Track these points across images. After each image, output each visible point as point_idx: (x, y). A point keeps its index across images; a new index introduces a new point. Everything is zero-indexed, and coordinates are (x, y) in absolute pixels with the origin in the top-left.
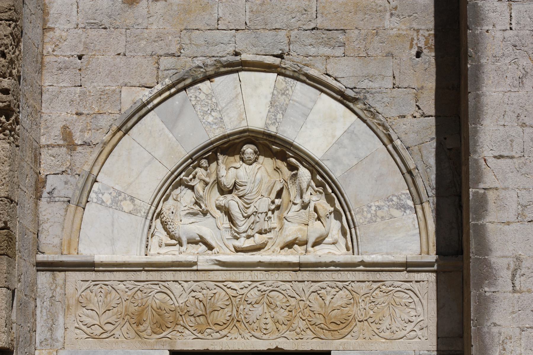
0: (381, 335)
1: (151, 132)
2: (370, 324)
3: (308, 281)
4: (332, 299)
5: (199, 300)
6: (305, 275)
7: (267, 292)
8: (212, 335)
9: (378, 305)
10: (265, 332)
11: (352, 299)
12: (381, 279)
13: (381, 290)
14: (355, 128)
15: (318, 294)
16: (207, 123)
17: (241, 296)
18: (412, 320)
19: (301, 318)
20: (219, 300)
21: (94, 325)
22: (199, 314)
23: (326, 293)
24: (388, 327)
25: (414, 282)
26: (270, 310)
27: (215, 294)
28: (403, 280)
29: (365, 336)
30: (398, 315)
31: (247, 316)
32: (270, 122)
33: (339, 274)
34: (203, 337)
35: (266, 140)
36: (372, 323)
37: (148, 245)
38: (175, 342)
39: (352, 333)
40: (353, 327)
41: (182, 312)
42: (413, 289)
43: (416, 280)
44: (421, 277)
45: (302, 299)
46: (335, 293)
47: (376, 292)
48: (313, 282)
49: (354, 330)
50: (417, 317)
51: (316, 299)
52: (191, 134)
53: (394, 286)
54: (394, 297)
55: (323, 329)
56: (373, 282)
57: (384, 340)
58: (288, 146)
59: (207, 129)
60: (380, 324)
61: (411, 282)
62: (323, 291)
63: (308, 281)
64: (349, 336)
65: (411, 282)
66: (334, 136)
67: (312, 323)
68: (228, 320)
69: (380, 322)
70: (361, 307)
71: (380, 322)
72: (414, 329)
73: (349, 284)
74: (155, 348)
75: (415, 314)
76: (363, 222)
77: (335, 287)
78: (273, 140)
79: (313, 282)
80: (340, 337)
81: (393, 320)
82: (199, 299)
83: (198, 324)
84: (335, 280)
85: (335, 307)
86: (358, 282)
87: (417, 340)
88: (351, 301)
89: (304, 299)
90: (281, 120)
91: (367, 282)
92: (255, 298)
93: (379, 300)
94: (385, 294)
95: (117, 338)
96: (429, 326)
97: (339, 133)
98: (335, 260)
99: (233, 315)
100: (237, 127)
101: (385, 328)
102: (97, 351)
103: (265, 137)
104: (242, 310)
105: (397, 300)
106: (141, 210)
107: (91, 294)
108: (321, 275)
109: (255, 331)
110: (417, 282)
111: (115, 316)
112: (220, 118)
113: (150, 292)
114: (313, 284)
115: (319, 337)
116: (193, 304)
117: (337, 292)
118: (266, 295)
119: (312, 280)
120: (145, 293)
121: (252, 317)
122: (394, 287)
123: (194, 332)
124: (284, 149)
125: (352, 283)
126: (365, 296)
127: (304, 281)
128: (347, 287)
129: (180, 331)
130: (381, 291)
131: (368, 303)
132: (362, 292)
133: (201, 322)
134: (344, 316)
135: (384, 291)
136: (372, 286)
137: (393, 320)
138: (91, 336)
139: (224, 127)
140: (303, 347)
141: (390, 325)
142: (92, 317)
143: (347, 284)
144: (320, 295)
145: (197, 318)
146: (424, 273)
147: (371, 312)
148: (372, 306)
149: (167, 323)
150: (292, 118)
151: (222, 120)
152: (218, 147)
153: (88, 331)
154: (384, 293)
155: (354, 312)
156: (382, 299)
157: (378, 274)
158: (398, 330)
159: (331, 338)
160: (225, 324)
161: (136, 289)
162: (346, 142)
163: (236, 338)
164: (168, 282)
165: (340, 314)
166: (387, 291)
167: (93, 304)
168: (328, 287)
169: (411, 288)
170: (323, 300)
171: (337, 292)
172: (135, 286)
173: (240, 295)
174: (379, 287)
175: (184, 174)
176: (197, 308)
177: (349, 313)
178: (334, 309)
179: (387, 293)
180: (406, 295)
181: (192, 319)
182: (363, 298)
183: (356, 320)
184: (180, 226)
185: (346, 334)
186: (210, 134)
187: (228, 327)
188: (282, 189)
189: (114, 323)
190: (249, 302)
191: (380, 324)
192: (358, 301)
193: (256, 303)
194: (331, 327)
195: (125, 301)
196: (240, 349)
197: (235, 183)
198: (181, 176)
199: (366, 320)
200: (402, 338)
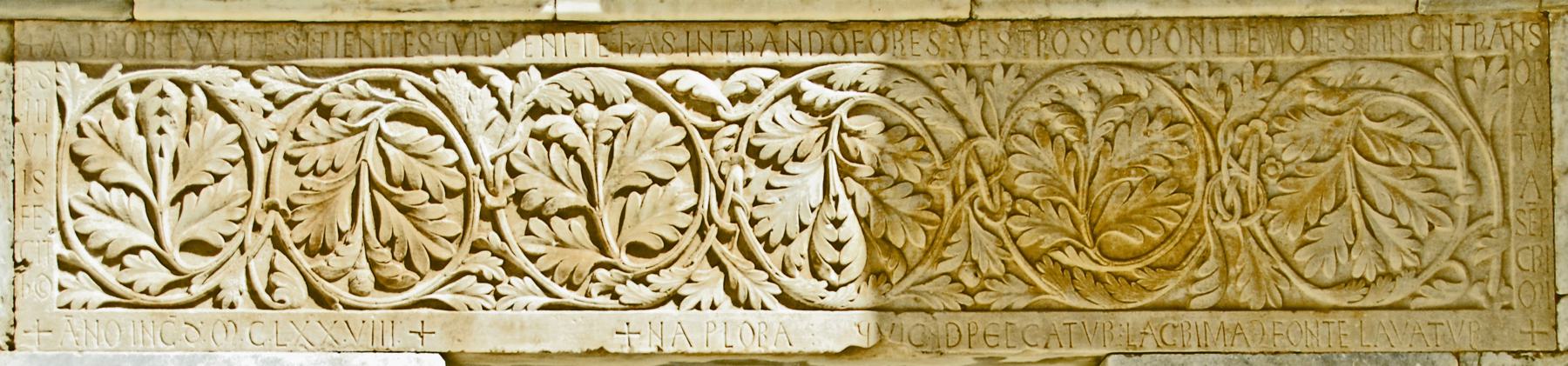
5: (564, 147)
7: (842, 111)
8: (619, 289)
10: (833, 277)
17: (734, 129)
20: (643, 146)
21: (135, 250)
22: (564, 205)
26: (854, 187)
27: (626, 120)
31: (758, 212)
33: (1136, 34)
34: (586, 302)
38: (469, 321)
41: (495, 194)
44: (1480, 38)
68: (683, 231)
74: (388, 344)
82: (565, 140)
83: (562, 244)
92: (792, 134)
95: (232, 306)
99: (703, 211)
102: (153, 357)
104: (740, 185)
107: (117, 122)
109: (796, 273)
111: (223, 215)
113: (366, 114)
116: (538, 163)
118: (836, 126)
120: (344, 118)
121: (778, 219)
123: (546, 281)
129: (488, 276)
133: (576, 240)
138: (117, 300)
142: (129, 220)
145: (556, 221)
149: (433, 240)
153: (110, 275)
160: (668, 246)
161: (306, 101)
163: (713, 307)
164: (437, 74)
167: (131, 161)
172: (301, 89)
173: (729, 123)
176: (556, 178)
181: (536, 224)
187: (683, 260)
189: (217, 241)
190: (764, 155)
193: (796, 158)
195: (263, 151)
196: (734, 350)
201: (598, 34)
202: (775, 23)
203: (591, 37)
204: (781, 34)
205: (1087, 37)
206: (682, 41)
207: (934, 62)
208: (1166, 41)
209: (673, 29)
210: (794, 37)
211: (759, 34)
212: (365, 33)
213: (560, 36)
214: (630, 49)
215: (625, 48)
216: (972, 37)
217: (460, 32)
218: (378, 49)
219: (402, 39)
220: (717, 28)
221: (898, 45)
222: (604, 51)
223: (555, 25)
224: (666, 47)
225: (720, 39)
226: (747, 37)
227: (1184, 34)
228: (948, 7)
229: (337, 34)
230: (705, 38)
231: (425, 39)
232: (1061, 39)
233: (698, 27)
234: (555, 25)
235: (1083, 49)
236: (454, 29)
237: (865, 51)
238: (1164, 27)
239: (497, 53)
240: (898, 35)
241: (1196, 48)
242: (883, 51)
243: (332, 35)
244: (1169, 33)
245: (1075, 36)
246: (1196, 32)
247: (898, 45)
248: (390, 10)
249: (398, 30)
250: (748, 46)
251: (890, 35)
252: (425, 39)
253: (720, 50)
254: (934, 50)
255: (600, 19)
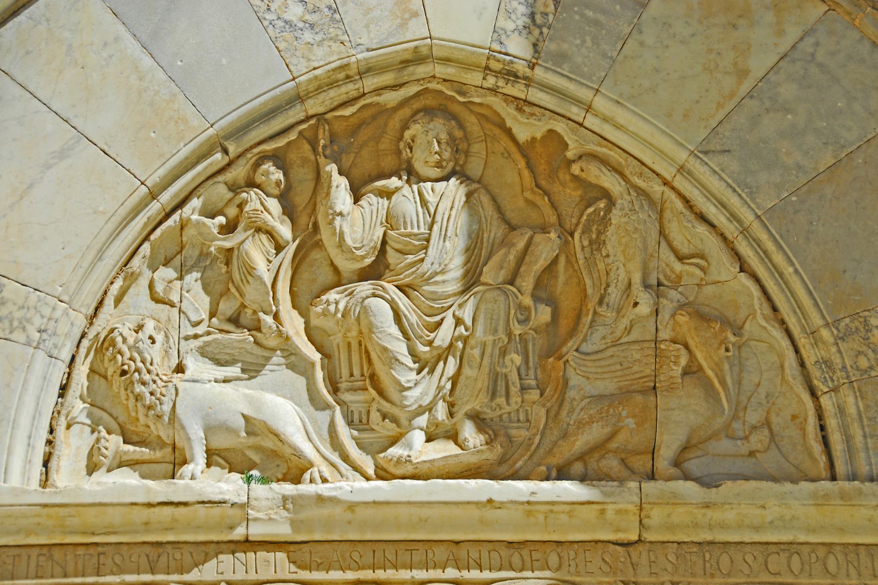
1: (70, 47)
14: (817, 44)
16: (280, 23)
32: (510, 26)
35: (494, 91)
37: (50, 453)
52: (224, 61)
58: (576, 112)
59: (282, 46)
66: (742, 73)
76: (871, 368)
78: (517, 90)
90: (551, 17)
97: (759, 64)
100: (393, 41)
103: (491, 81)
106: (29, 321)
112: (330, 8)
124: (560, 127)
139: (346, 38)
150: (590, 14)
151: (337, 16)
152: (320, 117)
162: (787, 91)
175: (196, 203)
184: (181, 386)
186: (294, 61)
188: (555, 261)
197: (384, 242)
198: (187, 210)
201: (288, 552)
202: (457, 543)
203: (281, 556)
204: (462, 552)
205: (749, 559)
206: (368, 558)
207: (606, 579)
208: (825, 564)
209: (359, 547)
210: (474, 555)
211: (441, 553)
212: (57, 553)
213: (251, 555)
214: (319, 567)
215: (314, 565)
216: (640, 555)
217: (153, 552)
218: (70, 568)
219: (95, 560)
220: (402, 546)
221: (573, 563)
222: (293, 568)
223: (248, 544)
224: (353, 564)
225: (406, 557)
226: (430, 555)
227: (841, 557)
228: (618, 530)
229: (29, 556)
230: (390, 556)
231: (118, 559)
232: (725, 560)
233: (384, 546)
234: (248, 544)
235: (746, 570)
236: (147, 549)
237: (542, 569)
238: (822, 552)
239: (189, 572)
240: (572, 553)
241: (853, 572)
242: (559, 568)
243: (25, 557)
244: (826, 557)
245: (738, 557)
246: (852, 557)
247: (573, 563)
248: (84, 533)
249: (92, 550)
250: (431, 564)
251: (564, 554)
252: (118, 559)
253: (405, 567)
254: (606, 569)
255: (290, 539)
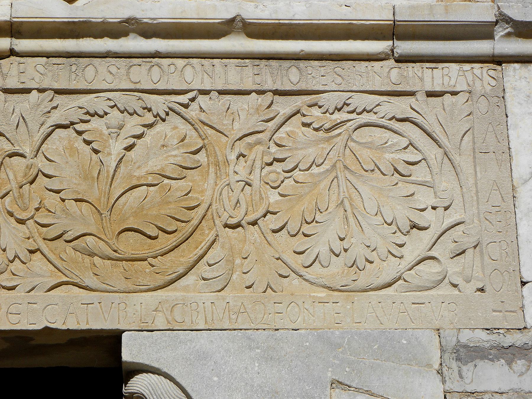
0: (308, 273)
2: (270, 237)
3: (41, 91)
4: (129, 148)
6: (30, 71)
9: (296, 173)
11: (203, 153)
12: (302, 86)
13: (307, 120)
15: (80, 133)
18: (422, 224)
19: (11, 214)
23: (106, 132)
24: (337, 246)
25: (421, 96)
28: (383, 89)
29: (249, 279)
30: (371, 207)
36: (275, 231)
39: (202, 268)
40: (204, 245)
42: (419, 120)
43: (429, 88)
44: (446, 79)
45: (17, 149)
46: (139, 130)
47: (286, 128)
48: (59, 92)
49: (210, 257)
50: (440, 210)
51: (72, 150)
53: (350, 108)
54: (351, 144)
55: (92, 254)
56: (276, 92)
57: (322, 294)
60: (306, 235)
61: (412, 94)
62: (95, 123)
63: (41, 91)
64: (190, 279)
65: (412, 94)
67: (53, 232)
69: (306, 229)
70: (237, 178)
71: (306, 229)
72: (432, 253)
73: (193, 100)
75: (432, 201)
77: (140, 111)
79: (59, 92)
80: (160, 283)
81: (351, 220)
84: (138, 86)
85: (139, 178)
86: (221, 92)
87: (445, 290)
88: (197, 157)
89: (27, 150)
91: (253, 94)
93: (300, 154)
94: (321, 134)
96: (485, 241)
98: (138, 15)
101: (324, 250)
105: (365, 154)
108: (90, 72)
110: (430, 94)
114: (59, 99)
115: (77, 280)
117: (150, 126)
119: (56, 86)
122: (349, 112)
125: (201, 99)
126: (250, 139)
127: (28, 91)
128: (182, 110)
130: (305, 125)
131: (258, 164)
132: (239, 128)
134: (171, 209)
135: (315, 125)
136: (273, 107)
137: (351, 220)
140: (14, 318)
141: (342, 239)
143: (184, 99)
144: (85, 136)
146: (454, 67)
147: (274, 197)
148: (273, 176)
154: (316, 130)
155: (209, 193)
156: (312, 153)
157: (294, 70)
158: (373, 256)
159: (122, 284)
165: (158, 199)
166: (327, 126)
168: (115, 113)
169: (413, 115)
170: (96, 152)
171: (150, 126)
174: (298, 112)
177: (191, 199)
178: (135, 182)
179: (328, 130)
180: (396, 138)
182: (240, 147)
183: (217, 222)
185: (181, 270)
191: (306, 235)
192: (220, 158)
194: (121, 247)
199: (254, 223)
200: (389, 285)
